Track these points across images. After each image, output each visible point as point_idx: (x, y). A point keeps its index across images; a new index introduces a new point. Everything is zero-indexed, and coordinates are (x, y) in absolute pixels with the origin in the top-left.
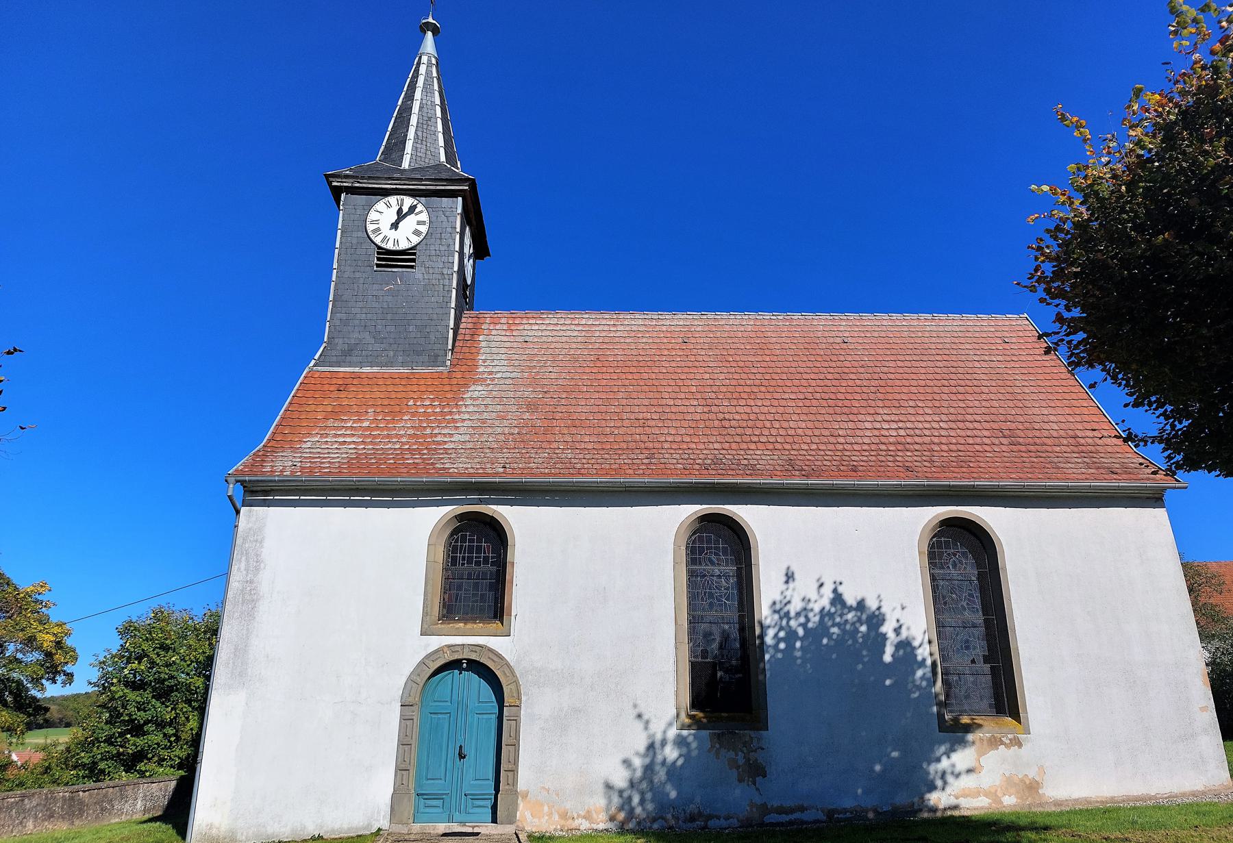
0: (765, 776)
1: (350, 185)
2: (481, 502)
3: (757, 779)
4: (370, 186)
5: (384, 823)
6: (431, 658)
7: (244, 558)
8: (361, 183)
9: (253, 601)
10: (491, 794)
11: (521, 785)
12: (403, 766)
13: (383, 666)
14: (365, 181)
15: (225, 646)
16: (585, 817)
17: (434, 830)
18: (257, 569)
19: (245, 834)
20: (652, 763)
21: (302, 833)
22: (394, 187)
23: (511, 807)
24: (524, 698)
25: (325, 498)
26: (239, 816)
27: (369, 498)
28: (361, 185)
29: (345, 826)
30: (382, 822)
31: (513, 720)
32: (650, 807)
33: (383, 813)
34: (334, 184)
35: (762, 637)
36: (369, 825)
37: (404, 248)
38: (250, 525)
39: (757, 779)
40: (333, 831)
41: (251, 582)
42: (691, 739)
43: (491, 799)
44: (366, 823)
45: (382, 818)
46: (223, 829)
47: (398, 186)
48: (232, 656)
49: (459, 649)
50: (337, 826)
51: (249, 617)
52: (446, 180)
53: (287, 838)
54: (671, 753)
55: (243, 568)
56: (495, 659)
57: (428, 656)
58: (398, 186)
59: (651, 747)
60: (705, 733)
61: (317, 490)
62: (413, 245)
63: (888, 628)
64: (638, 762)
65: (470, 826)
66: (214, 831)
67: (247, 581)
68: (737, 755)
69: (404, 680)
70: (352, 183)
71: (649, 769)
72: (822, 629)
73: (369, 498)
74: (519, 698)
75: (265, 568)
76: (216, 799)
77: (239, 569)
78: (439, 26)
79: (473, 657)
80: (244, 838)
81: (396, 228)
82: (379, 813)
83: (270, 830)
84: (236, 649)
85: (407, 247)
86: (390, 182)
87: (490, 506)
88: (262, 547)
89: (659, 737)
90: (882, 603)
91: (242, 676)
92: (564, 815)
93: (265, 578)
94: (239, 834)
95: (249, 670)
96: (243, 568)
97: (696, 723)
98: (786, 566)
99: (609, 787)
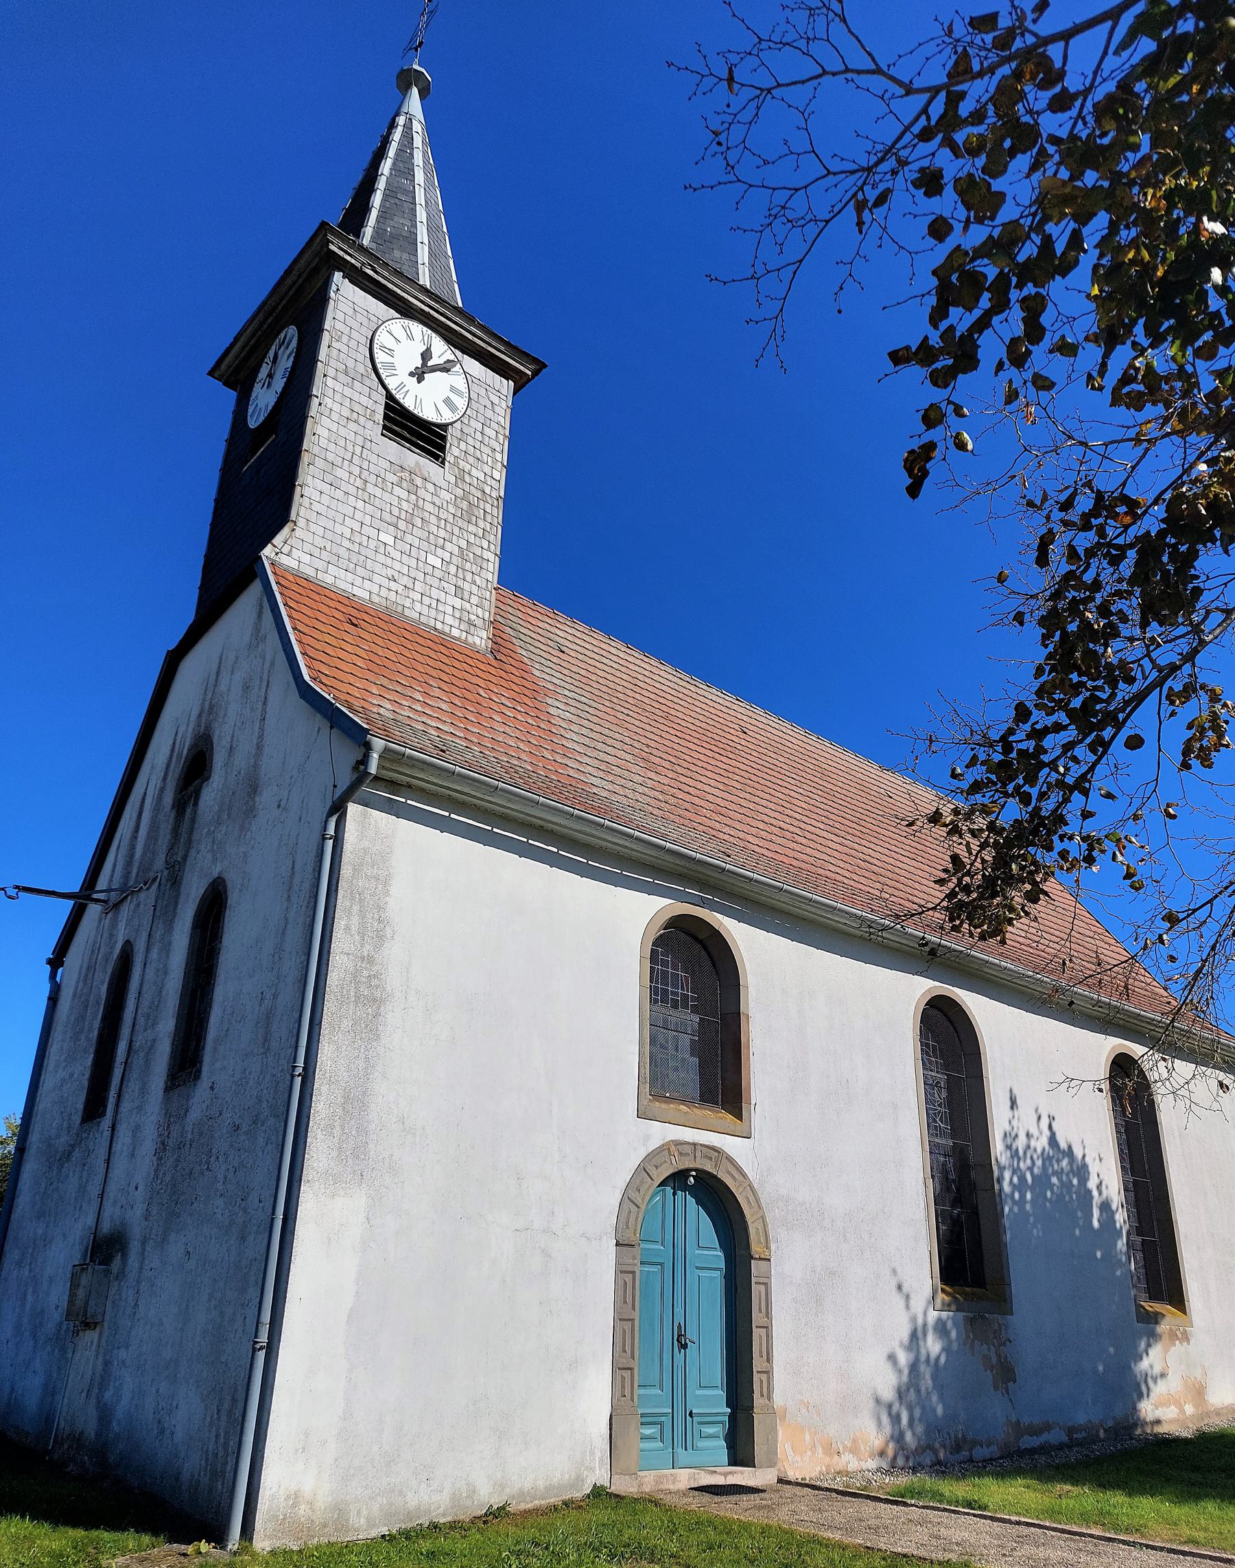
0: (1015, 1382)
1: (358, 265)
2: (702, 903)
3: (1009, 1384)
4: (390, 286)
5: (599, 1475)
6: (654, 1162)
7: (356, 908)
8: (376, 272)
9: (375, 1000)
10: (723, 1414)
11: (778, 1399)
12: (624, 1362)
13: (585, 1166)
14: (386, 274)
15: (325, 1089)
16: (851, 1451)
17: (674, 1483)
18: (380, 938)
19: (365, 1512)
20: (917, 1360)
21: (469, 1503)
22: (427, 309)
23: (770, 1437)
24: (773, 1247)
25: (490, 828)
26: (352, 1471)
27: (556, 850)
28: (376, 276)
29: (541, 1484)
30: (598, 1472)
31: (763, 1283)
32: (920, 1429)
33: (598, 1455)
34: (332, 247)
35: (1000, 1180)
36: (579, 1480)
37: (430, 419)
38: (366, 844)
39: (1009, 1384)
40: (522, 1495)
41: (370, 960)
42: (950, 1324)
43: (721, 1422)
44: (574, 1475)
45: (597, 1466)
46: (320, 1504)
47: (432, 312)
48: (339, 1111)
49: (688, 1149)
50: (527, 1485)
51: (370, 1030)
52: (507, 344)
53: (444, 1515)
54: (933, 1346)
55: (354, 929)
56: (735, 1173)
57: (650, 1157)
58: (432, 312)
59: (914, 1335)
60: (961, 1315)
61: (478, 808)
62: (444, 421)
63: (1092, 1184)
64: (903, 1358)
65: (721, 1474)
66: (303, 1510)
67: (363, 958)
68: (989, 1350)
69: (618, 1196)
70: (363, 264)
71: (914, 1367)
72: (1041, 1181)
73: (556, 850)
74: (768, 1247)
75: (393, 938)
76: (307, 1434)
77: (347, 928)
78: (430, 79)
79: (709, 1167)
80: (362, 1521)
81: (420, 380)
82: (592, 1453)
83: (412, 1501)
84: (346, 1098)
85: (434, 420)
86: (422, 297)
87: (715, 913)
88: (387, 893)
89: (920, 1321)
90: (1086, 1151)
91: (358, 1157)
92: (831, 1450)
93: (394, 953)
94: (353, 1513)
95: (371, 1146)
96: (354, 929)
97: (955, 1304)
98: (1009, 1089)
99: (878, 1401)
